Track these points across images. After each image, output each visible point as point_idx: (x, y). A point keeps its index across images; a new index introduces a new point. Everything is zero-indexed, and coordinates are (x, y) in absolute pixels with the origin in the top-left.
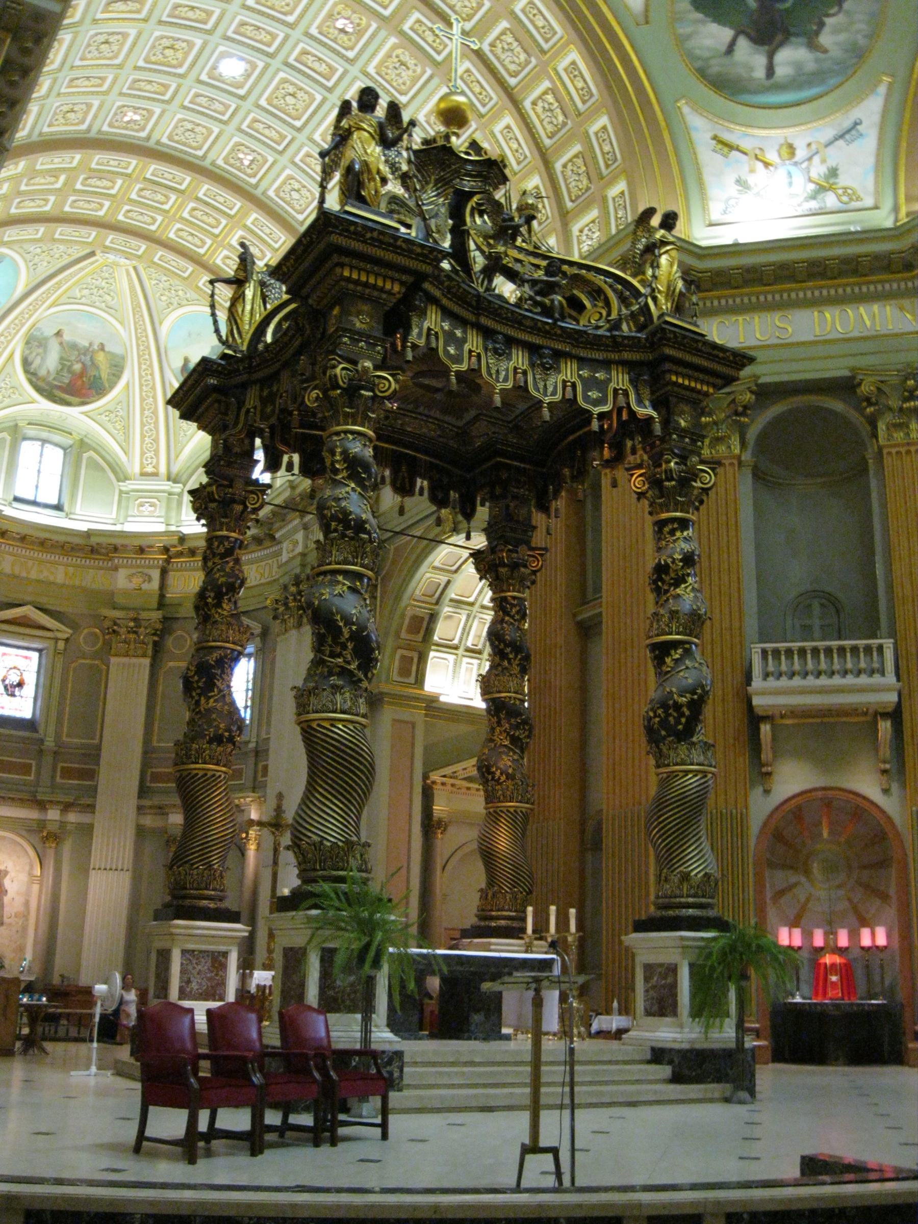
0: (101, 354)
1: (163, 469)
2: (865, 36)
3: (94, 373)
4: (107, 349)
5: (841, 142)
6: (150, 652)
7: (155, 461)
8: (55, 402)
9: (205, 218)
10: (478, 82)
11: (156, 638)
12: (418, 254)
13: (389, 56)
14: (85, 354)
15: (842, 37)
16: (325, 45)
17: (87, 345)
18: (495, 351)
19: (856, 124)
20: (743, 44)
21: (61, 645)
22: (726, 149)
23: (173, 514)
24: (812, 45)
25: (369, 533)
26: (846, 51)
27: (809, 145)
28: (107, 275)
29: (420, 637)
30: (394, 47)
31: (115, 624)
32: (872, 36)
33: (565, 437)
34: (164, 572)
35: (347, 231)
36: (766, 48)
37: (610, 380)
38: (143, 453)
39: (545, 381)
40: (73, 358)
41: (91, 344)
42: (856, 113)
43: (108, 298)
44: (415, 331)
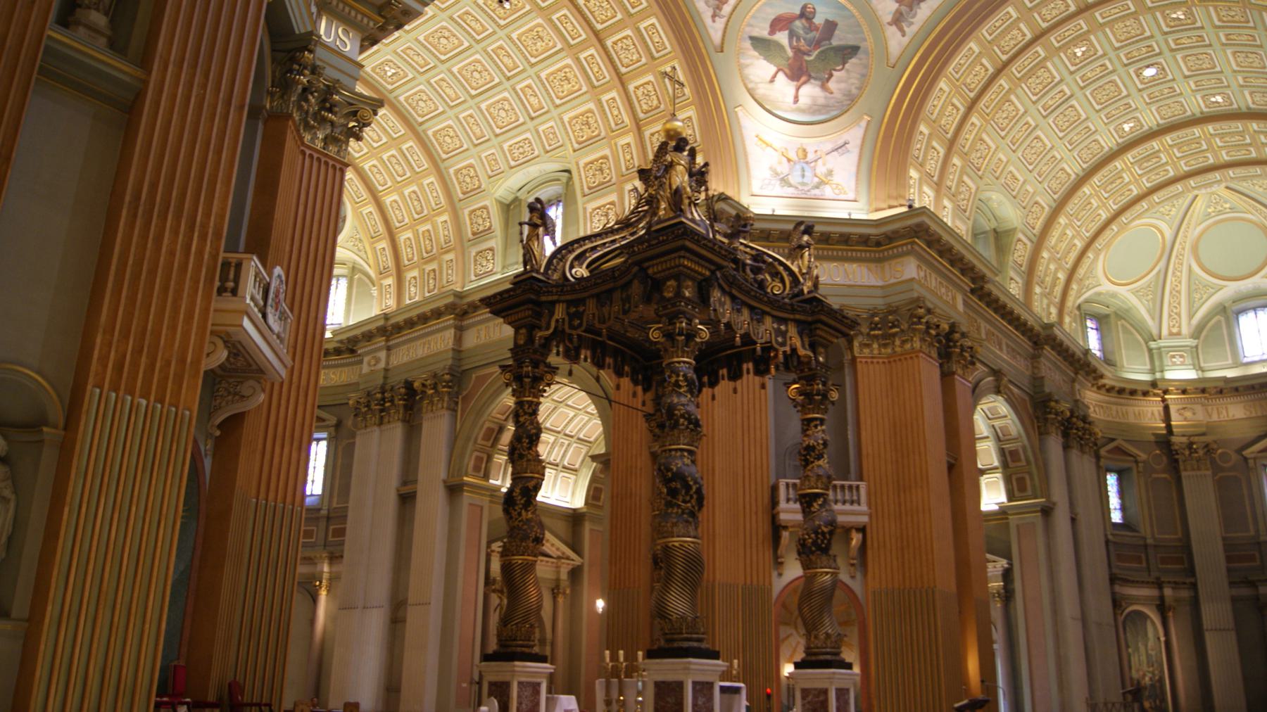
2: (856, 88)
5: (835, 153)
10: (598, 64)
13: (531, 30)
15: (843, 86)
19: (846, 143)
20: (781, 76)
22: (764, 145)
24: (824, 87)
26: (844, 95)
27: (816, 151)
29: (490, 444)
32: (860, 88)
33: (726, 350)
36: (795, 83)
42: (846, 136)
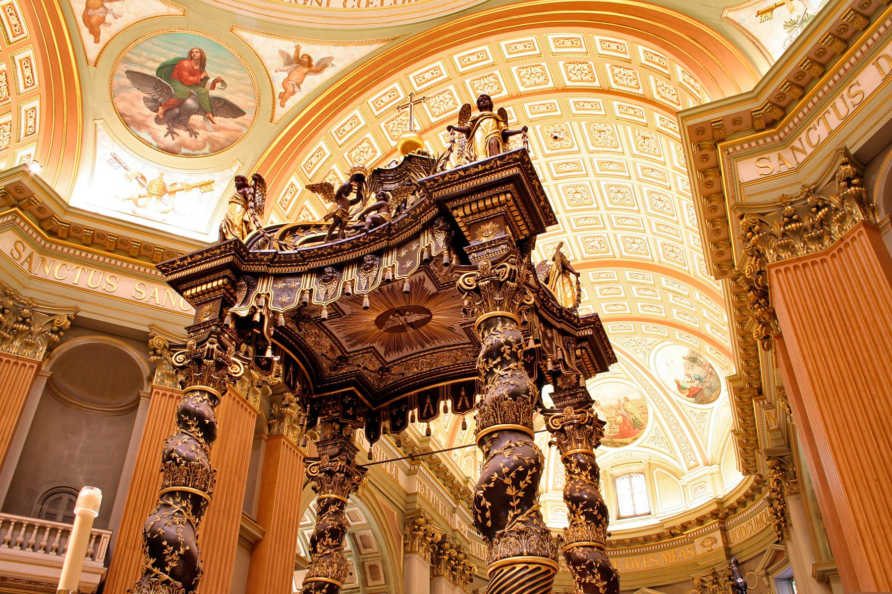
0: (629, 403)
1: (700, 461)
7: (692, 456)
8: (617, 446)
9: (610, 291)
14: (619, 409)
16: (559, 154)
22: (769, 14)
30: (588, 126)
31: (702, 580)
34: (724, 531)
38: (684, 455)
40: (614, 415)
41: (619, 401)
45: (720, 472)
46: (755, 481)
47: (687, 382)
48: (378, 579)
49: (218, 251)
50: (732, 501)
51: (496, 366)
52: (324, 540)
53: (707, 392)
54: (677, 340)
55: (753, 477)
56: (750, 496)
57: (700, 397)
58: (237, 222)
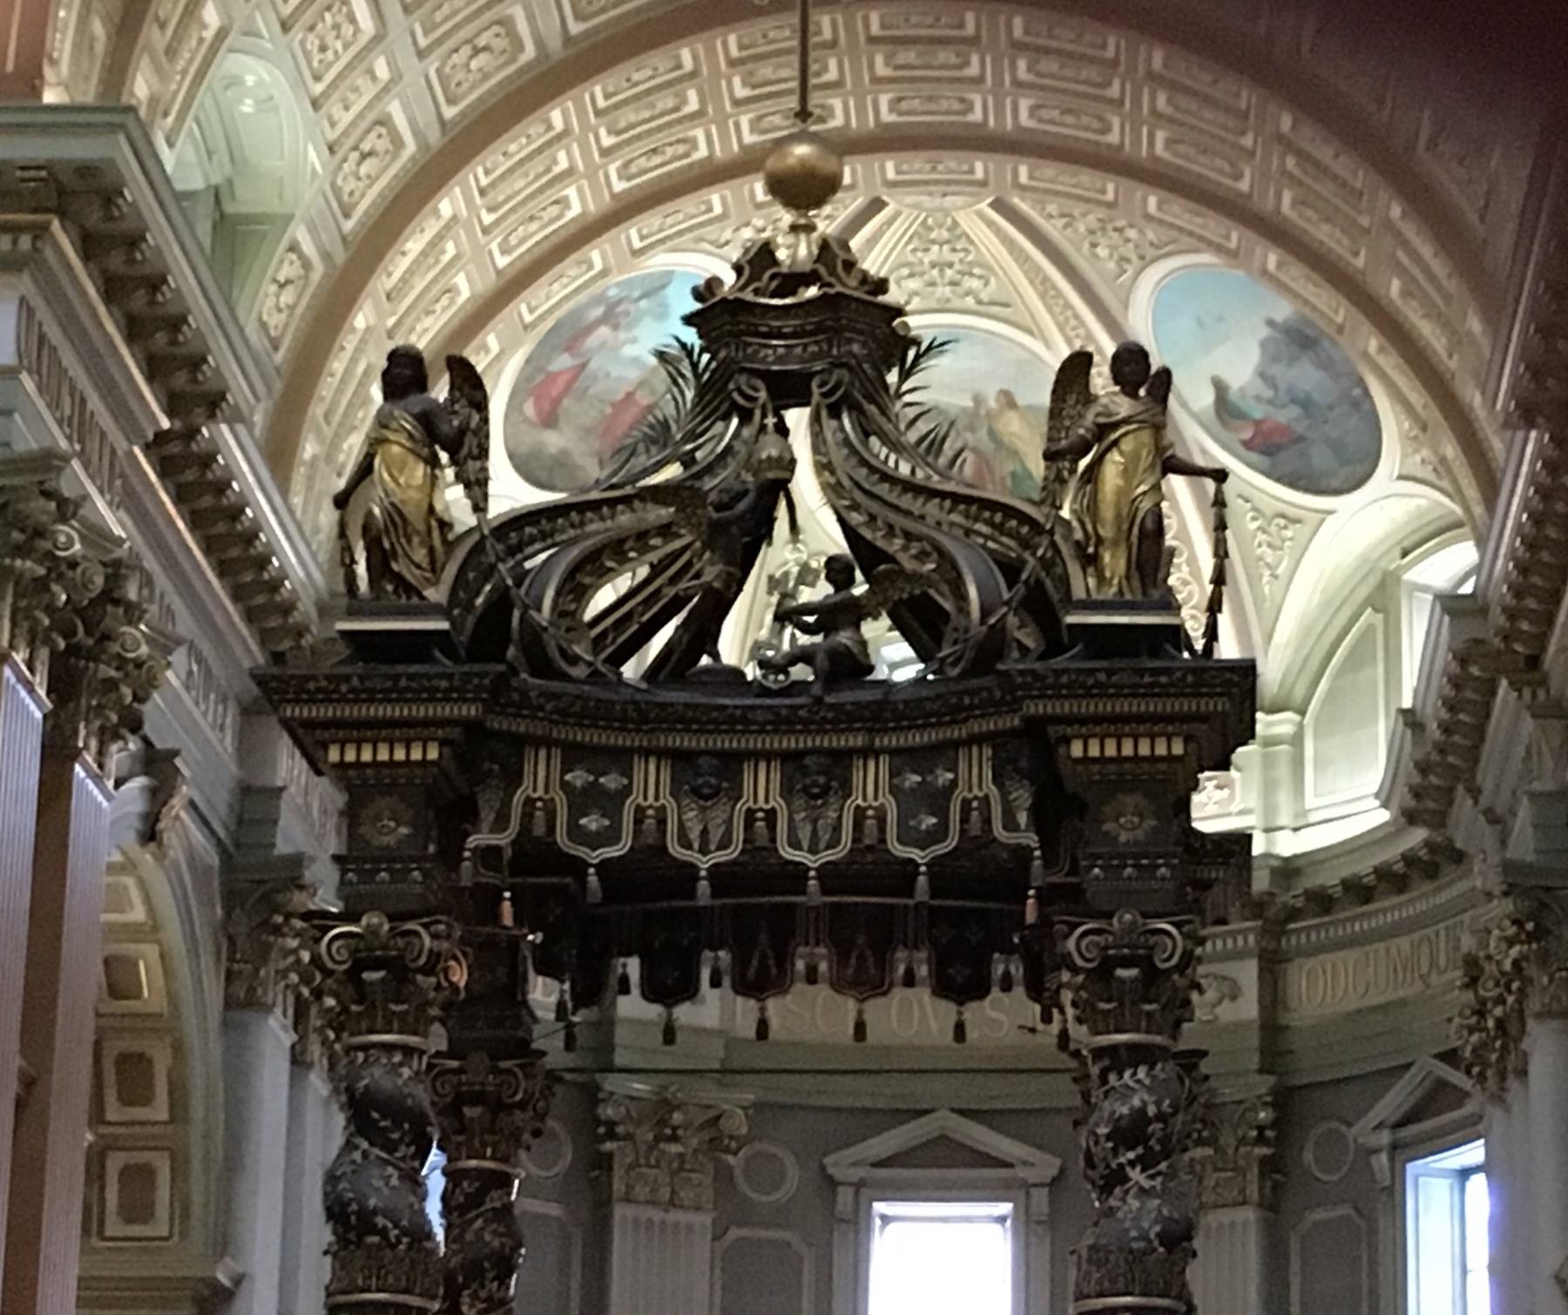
3: (1009, 466)
4: (1021, 401)
6: (1253, 1191)
11: (1265, 1151)
12: (447, 691)
17: (970, 404)
18: (696, 792)
21: (1041, 1197)
23: (1283, 797)
25: (383, 1233)
28: (945, 235)
34: (1272, 965)
35: (308, 692)
37: (954, 783)
39: (815, 821)
41: (978, 400)
43: (975, 284)
44: (487, 817)
45: (1297, 740)
46: (1427, 844)
47: (1258, 398)
48: (146, 1100)
49: (444, 684)
50: (1330, 878)
51: (1132, 1163)
52: (483, 1286)
53: (1320, 457)
54: (1264, 272)
55: (1418, 836)
56: (1393, 879)
57: (1288, 459)
58: (415, 516)
